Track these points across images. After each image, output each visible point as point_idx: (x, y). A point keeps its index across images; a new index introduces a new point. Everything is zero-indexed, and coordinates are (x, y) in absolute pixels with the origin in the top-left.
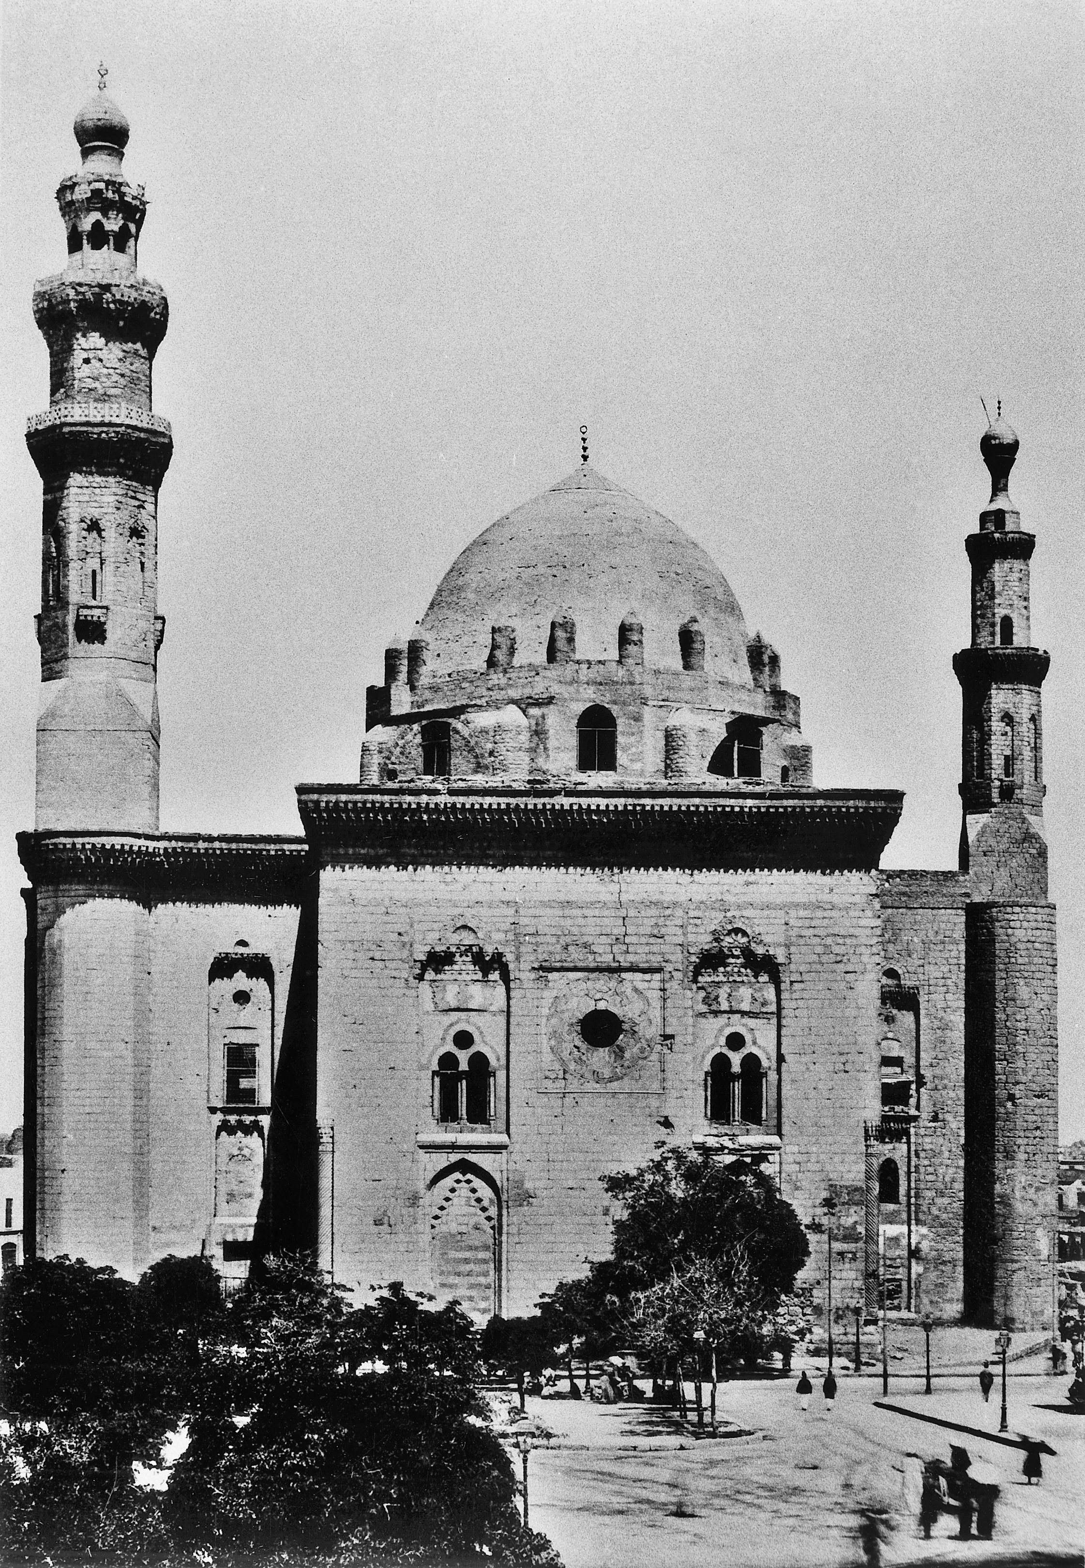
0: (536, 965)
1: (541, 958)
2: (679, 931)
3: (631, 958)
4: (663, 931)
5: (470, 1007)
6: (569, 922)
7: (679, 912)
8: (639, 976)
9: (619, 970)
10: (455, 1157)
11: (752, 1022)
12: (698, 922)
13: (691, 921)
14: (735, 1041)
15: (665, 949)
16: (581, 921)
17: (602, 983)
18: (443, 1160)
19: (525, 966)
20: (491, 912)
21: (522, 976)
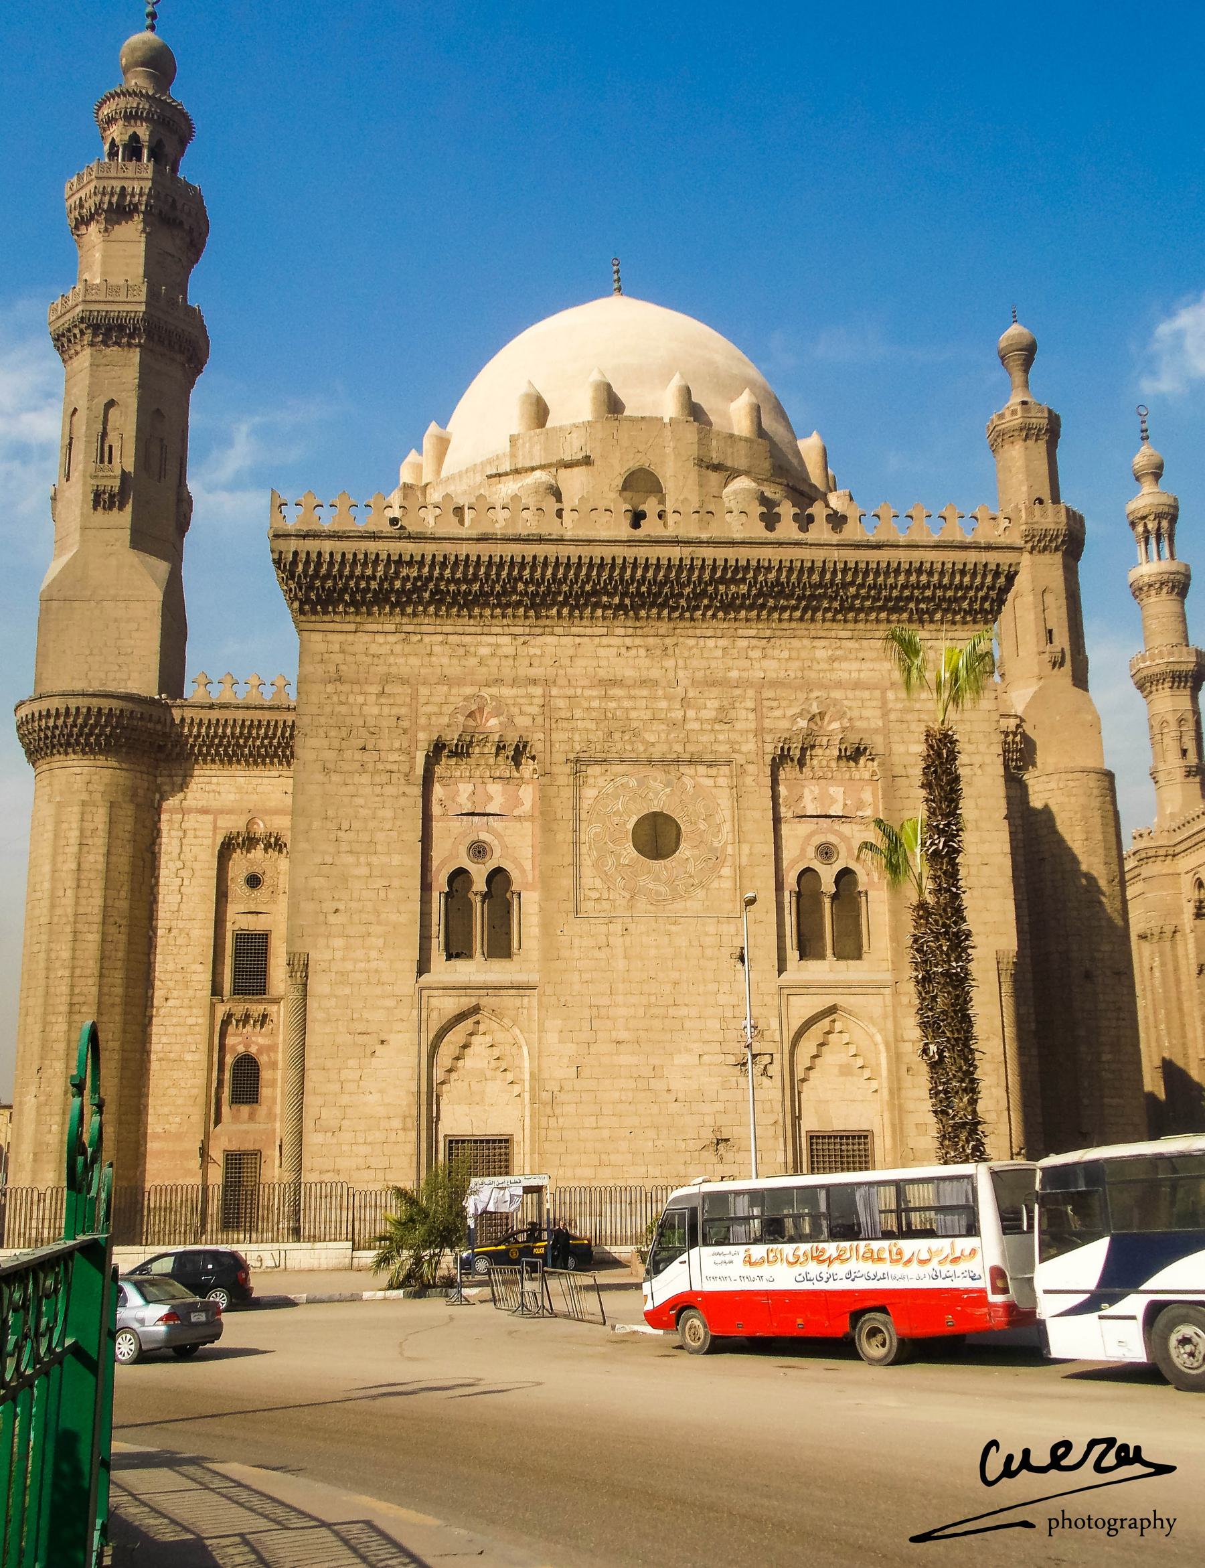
0: (572, 756)
1: (578, 748)
2: (752, 716)
3: (691, 748)
4: (732, 714)
5: (488, 811)
6: (612, 705)
7: (751, 693)
8: (702, 769)
9: (677, 762)
10: (466, 1003)
11: (846, 828)
12: (775, 704)
13: (764, 702)
14: (826, 852)
15: (733, 736)
16: (626, 704)
17: (657, 779)
18: (450, 1005)
19: (559, 757)
20: (514, 691)
21: (555, 769)
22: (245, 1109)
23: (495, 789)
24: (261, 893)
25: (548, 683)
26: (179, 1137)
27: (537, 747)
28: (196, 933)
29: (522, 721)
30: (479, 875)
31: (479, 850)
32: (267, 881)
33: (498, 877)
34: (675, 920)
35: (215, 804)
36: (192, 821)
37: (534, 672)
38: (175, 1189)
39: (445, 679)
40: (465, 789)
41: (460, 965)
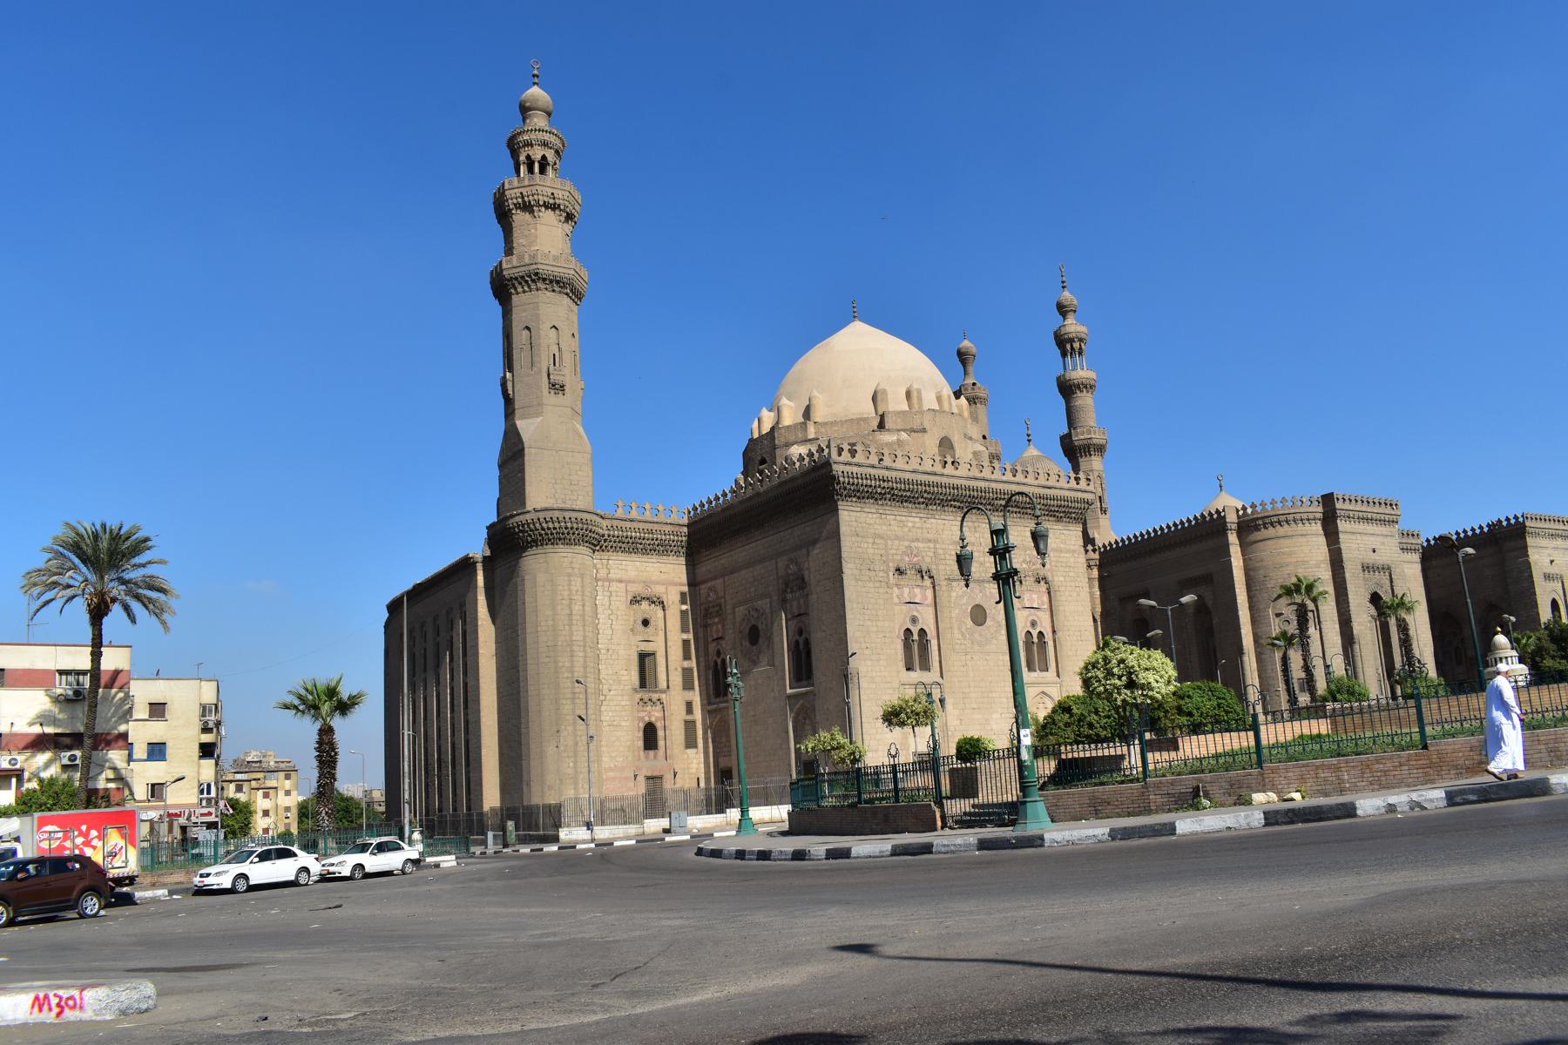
14: (1033, 624)
22: (651, 753)
23: (917, 591)
24: (650, 629)
25: (936, 542)
26: (623, 769)
27: (934, 573)
28: (622, 652)
29: (928, 560)
30: (915, 631)
31: (914, 620)
32: (652, 622)
33: (922, 632)
34: (988, 653)
35: (625, 577)
36: (615, 586)
37: (930, 536)
38: (623, 798)
39: (897, 538)
40: (906, 590)
41: (912, 674)
